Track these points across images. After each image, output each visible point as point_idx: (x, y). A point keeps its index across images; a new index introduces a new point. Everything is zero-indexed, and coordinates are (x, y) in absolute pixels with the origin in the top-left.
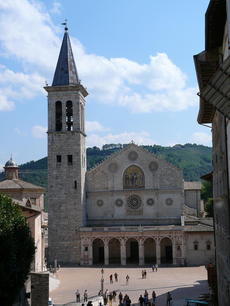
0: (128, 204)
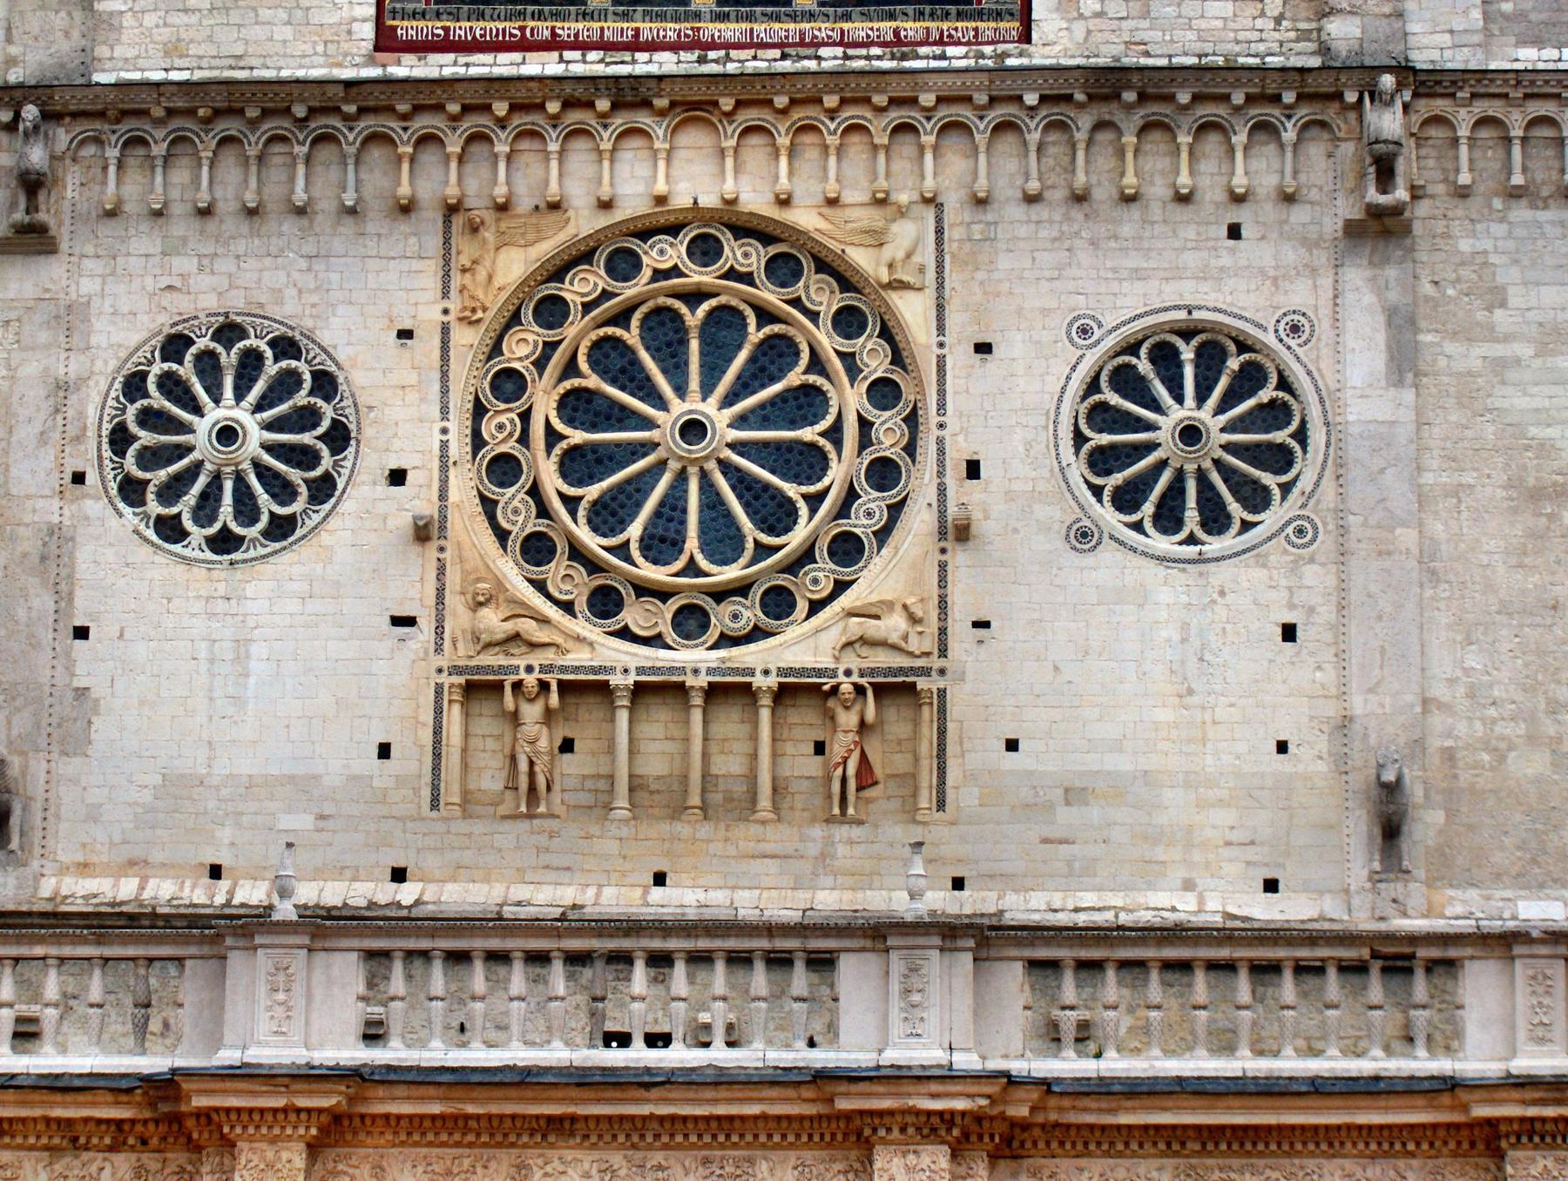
0: (504, 469)
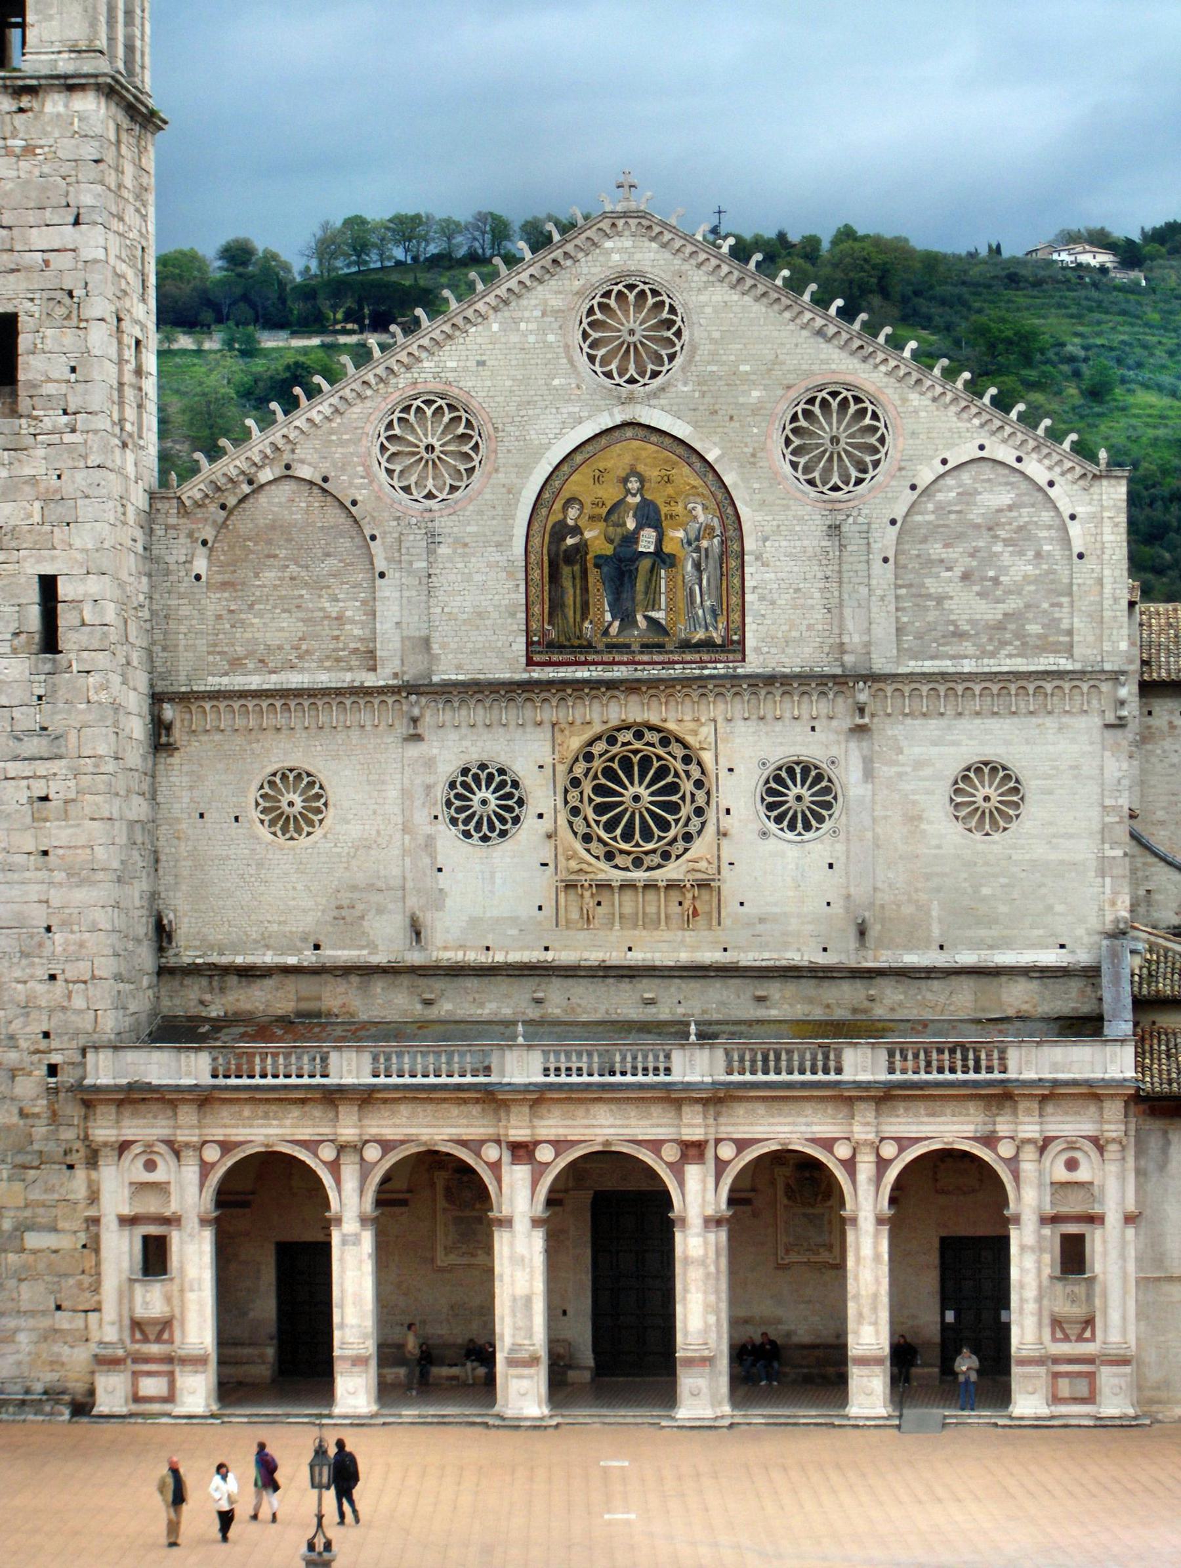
0: (575, 811)
